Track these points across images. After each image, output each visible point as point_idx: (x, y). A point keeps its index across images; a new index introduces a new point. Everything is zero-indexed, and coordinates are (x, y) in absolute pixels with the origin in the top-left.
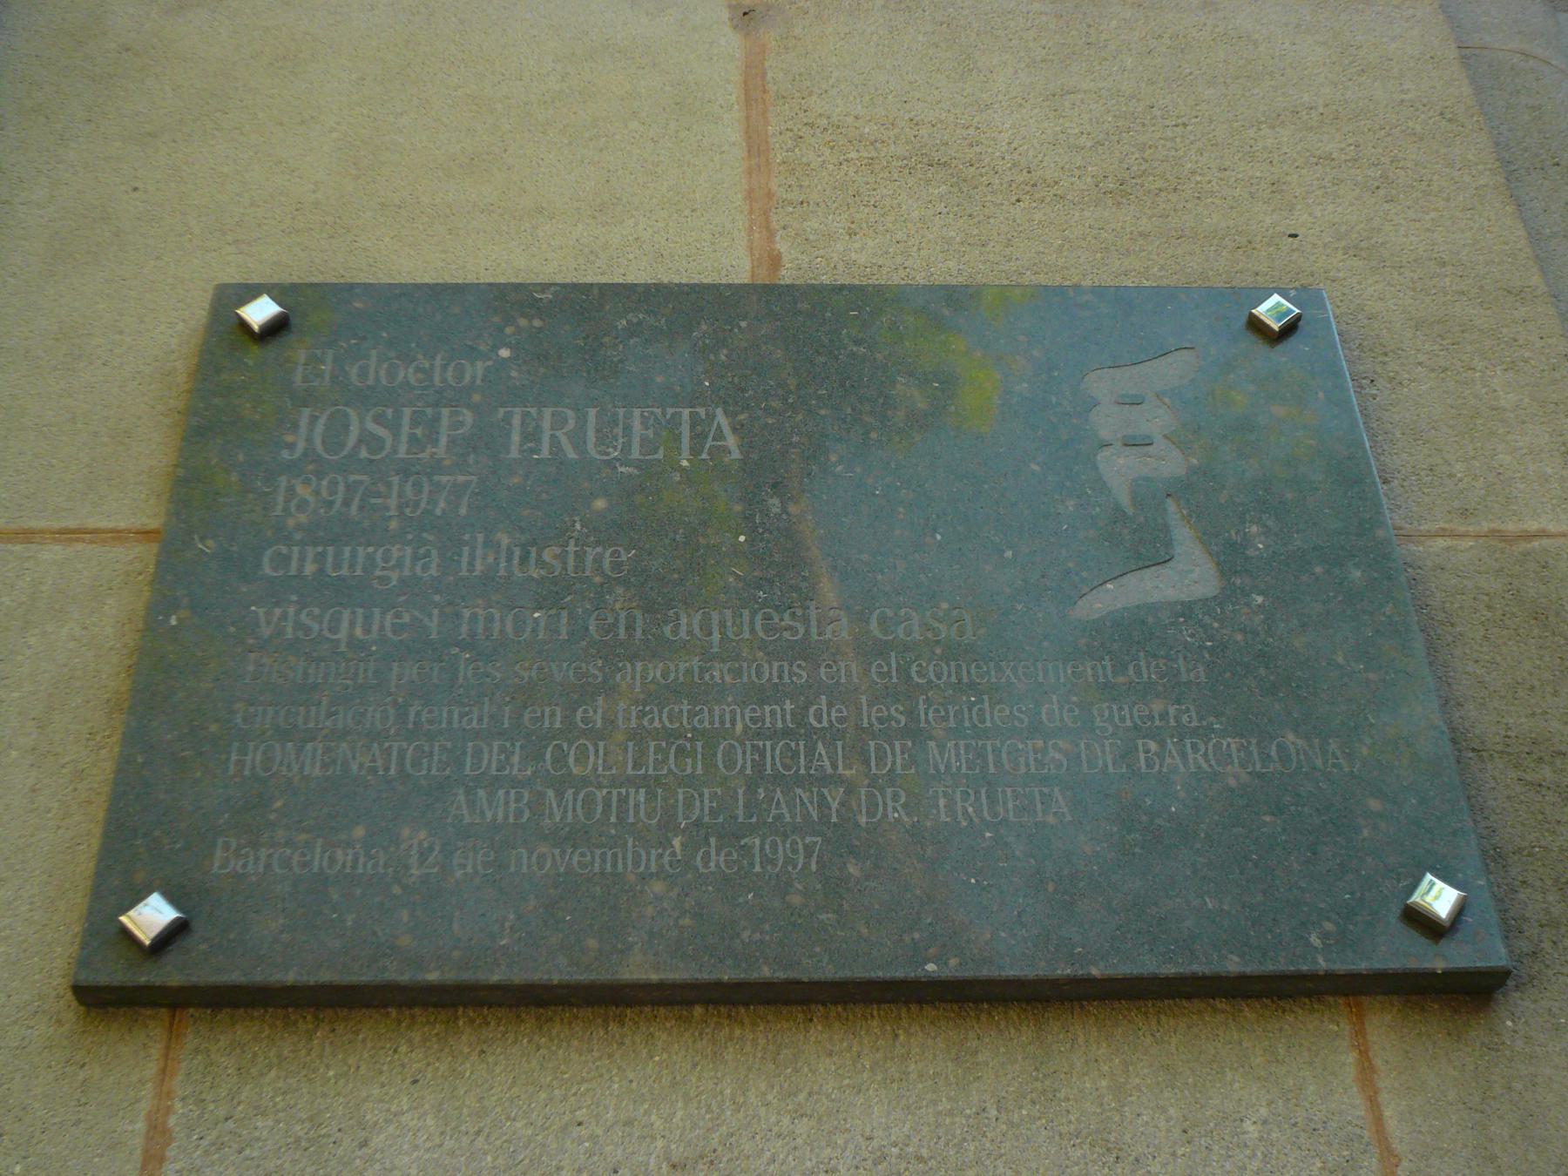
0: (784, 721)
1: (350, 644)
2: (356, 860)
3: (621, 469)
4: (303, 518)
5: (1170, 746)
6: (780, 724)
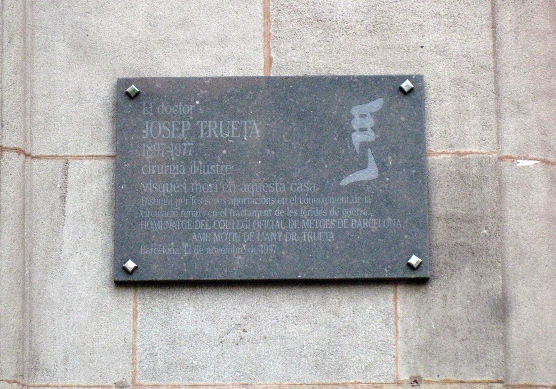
0: (269, 214)
1: (165, 194)
2: (172, 251)
3: (229, 141)
4: (150, 157)
5: (360, 221)
6: (268, 216)
